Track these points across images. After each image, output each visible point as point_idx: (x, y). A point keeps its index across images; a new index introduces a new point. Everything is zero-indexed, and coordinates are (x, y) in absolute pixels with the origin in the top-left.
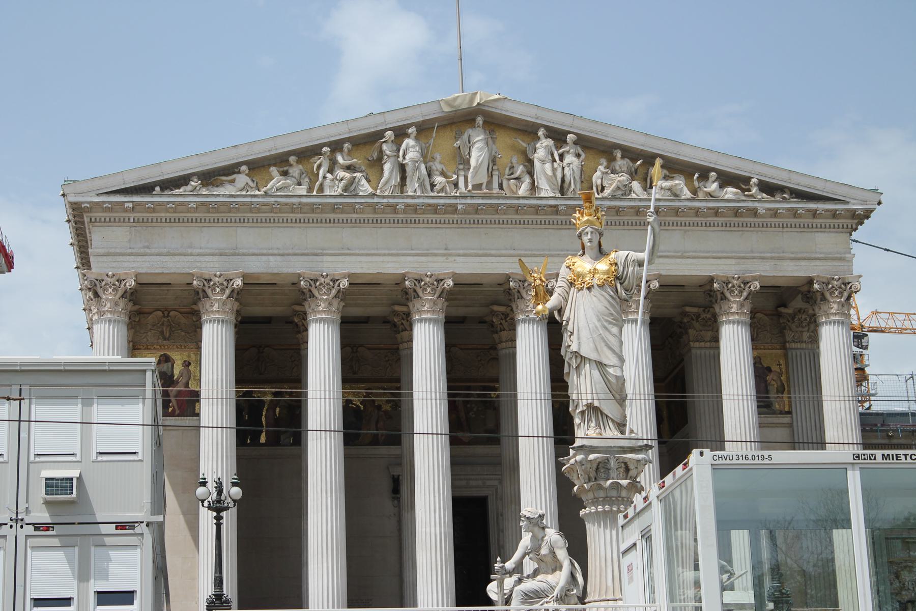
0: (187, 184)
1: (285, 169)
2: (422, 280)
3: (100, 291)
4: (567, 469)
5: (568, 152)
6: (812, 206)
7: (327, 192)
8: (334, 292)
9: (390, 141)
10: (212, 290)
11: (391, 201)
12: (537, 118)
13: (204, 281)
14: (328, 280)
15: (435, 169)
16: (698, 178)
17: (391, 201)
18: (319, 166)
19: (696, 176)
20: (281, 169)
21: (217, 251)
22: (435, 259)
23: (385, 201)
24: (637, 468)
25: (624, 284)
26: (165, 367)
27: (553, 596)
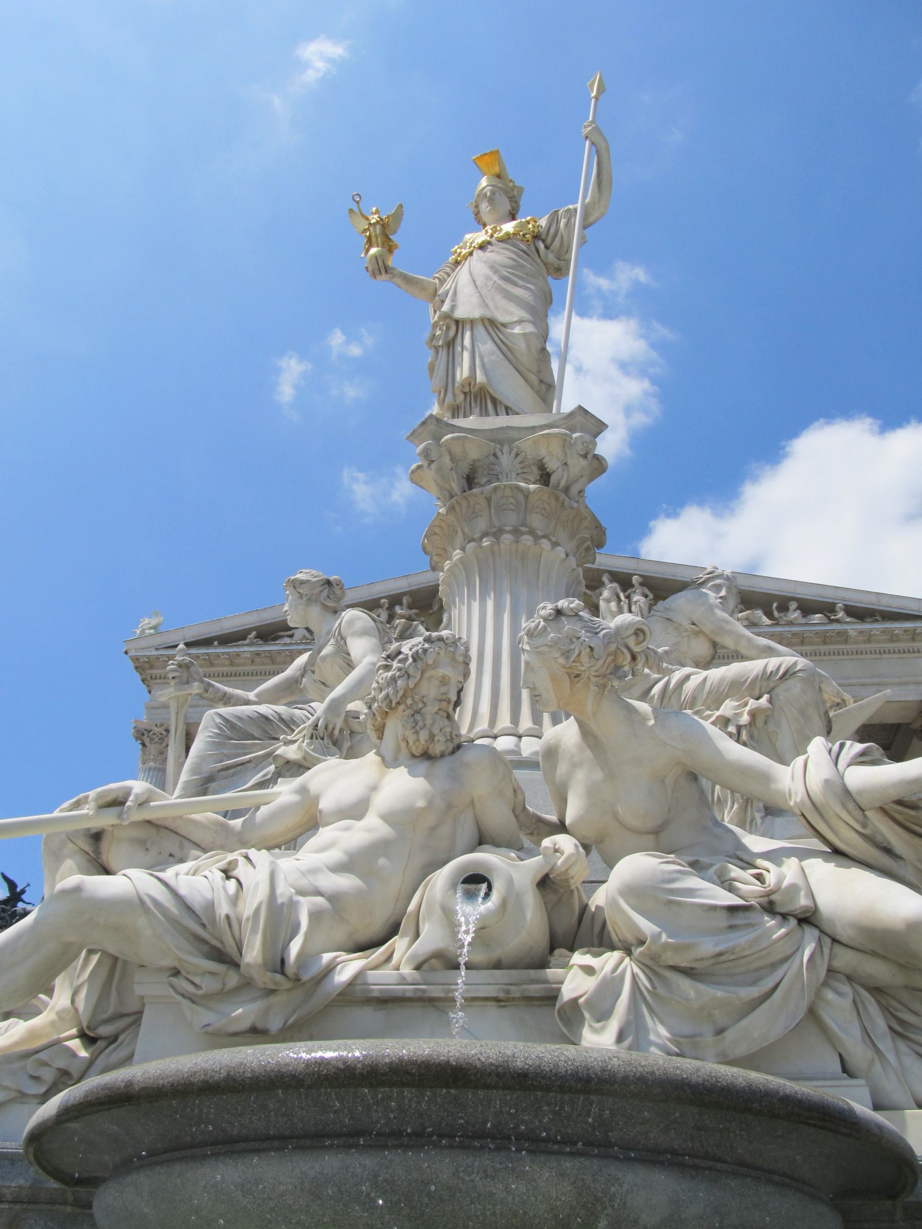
0: (245, 638)
3: (147, 741)
5: (635, 592)
6: (908, 625)
12: (600, 565)
16: (777, 608)
19: (775, 605)
24: (565, 464)
25: (552, 248)
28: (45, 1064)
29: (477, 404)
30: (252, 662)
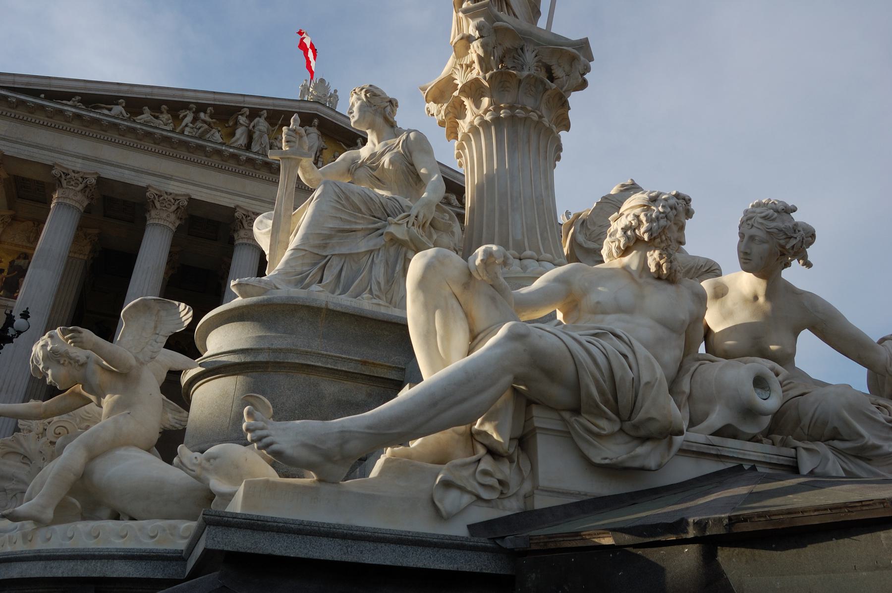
1: (157, 114)
2: (249, 216)
4: (433, 89)
7: (186, 133)
8: (173, 208)
9: (245, 115)
10: (67, 182)
11: (235, 151)
13: (62, 173)
14: (170, 198)
15: (276, 145)
17: (235, 151)
18: (185, 116)
20: (152, 113)
21: (81, 155)
22: (263, 204)
23: (231, 150)
26: (21, 262)
27: (409, 215)
28: (485, 473)
29: (495, 3)
30: (72, 120)
